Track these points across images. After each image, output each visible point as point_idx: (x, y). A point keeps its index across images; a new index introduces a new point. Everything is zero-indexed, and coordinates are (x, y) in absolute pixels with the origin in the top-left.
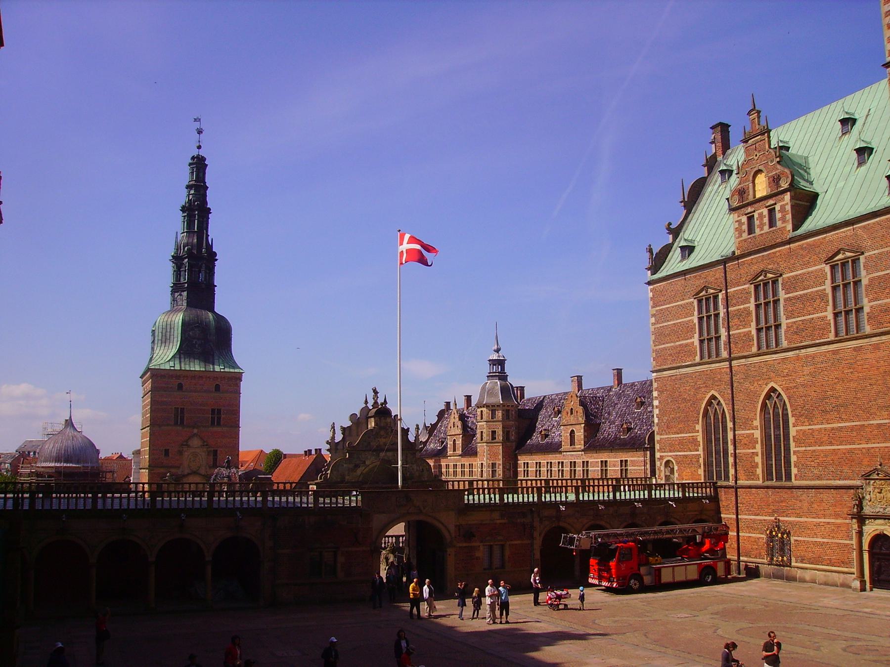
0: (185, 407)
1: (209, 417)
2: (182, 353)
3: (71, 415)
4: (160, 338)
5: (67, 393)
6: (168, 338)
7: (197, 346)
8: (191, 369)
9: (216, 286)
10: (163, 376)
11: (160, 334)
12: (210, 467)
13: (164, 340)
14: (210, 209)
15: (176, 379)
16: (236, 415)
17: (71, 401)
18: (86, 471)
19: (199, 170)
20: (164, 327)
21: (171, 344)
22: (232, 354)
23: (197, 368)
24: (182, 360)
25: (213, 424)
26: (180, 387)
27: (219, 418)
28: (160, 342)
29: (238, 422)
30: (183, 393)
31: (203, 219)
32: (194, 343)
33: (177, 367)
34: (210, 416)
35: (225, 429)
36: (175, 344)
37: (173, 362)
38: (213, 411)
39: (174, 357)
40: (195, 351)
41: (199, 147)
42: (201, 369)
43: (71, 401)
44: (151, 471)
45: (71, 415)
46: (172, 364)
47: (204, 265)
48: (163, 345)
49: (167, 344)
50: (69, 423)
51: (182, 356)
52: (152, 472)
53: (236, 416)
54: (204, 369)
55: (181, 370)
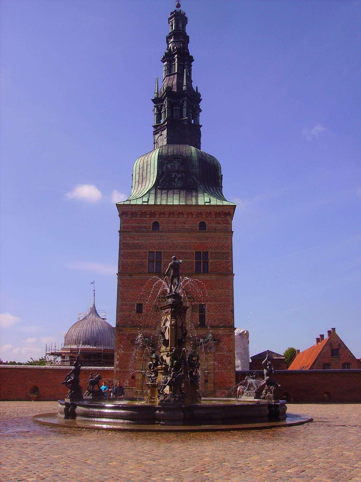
0: (163, 251)
2: (159, 189)
3: (94, 303)
4: (137, 180)
5: (92, 283)
6: (145, 177)
7: (176, 179)
8: (169, 204)
9: (201, 126)
10: (134, 214)
11: (137, 175)
12: (196, 327)
13: (141, 180)
14: (192, 57)
15: (150, 217)
17: (94, 291)
18: (100, 352)
20: (141, 166)
21: (148, 182)
22: (223, 196)
23: (176, 202)
24: (159, 195)
25: (198, 272)
26: (156, 225)
27: (206, 263)
28: (137, 184)
29: (230, 268)
30: (160, 234)
31: (184, 63)
32: (173, 176)
33: (152, 202)
34: (194, 260)
35: (214, 277)
36: (151, 180)
37: (147, 198)
39: (149, 192)
41: (178, 6)
42: (181, 204)
43: (94, 291)
44: (119, 331)
45: (94, 303)
46: (145, 199)
47: (185, 102)
48: (140, 185)
49: (144, 184)
50: (94, 311)
52: (120, 333)
54: (184, 204)
55: (155, 205)
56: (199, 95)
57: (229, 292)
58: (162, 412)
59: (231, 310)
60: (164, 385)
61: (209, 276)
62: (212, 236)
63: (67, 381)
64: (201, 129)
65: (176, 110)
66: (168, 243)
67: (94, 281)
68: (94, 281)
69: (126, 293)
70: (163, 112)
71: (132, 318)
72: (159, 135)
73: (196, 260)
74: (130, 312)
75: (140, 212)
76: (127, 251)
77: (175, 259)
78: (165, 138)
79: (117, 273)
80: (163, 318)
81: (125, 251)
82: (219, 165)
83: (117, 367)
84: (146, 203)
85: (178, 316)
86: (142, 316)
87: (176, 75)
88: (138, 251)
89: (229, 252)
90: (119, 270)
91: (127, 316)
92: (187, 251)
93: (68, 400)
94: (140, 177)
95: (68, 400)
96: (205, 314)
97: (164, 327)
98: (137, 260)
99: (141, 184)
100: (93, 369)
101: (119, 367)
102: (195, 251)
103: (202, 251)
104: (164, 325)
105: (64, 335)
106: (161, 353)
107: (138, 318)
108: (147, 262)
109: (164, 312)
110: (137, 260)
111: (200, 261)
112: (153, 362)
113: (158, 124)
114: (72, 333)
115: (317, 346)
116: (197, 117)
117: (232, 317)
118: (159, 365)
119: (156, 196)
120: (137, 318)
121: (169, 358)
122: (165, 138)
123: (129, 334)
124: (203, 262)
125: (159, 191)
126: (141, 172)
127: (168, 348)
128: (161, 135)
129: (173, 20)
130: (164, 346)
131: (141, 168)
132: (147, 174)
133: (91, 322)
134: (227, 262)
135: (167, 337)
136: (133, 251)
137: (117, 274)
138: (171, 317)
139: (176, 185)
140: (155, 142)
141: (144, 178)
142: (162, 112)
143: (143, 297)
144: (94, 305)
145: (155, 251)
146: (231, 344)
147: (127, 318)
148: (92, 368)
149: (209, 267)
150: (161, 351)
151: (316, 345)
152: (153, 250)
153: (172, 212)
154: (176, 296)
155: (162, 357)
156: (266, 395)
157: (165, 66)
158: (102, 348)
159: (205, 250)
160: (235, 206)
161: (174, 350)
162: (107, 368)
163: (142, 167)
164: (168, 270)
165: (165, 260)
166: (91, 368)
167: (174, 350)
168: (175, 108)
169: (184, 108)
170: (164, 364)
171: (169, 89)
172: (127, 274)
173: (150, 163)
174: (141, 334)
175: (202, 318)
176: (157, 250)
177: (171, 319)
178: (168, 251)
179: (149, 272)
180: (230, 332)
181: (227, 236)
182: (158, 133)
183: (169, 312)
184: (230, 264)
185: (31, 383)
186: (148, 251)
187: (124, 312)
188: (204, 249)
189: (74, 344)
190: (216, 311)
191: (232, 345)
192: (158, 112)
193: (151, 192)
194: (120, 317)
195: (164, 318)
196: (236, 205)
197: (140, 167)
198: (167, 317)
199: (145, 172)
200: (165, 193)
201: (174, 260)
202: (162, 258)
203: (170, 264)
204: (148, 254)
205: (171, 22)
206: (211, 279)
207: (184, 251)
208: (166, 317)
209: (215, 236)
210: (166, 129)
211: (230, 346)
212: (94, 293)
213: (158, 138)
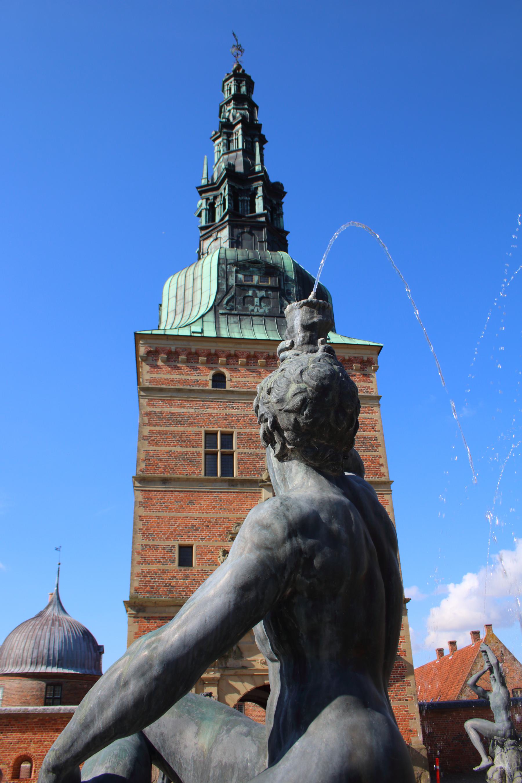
4: (172, 307)
14: (263, 136)
19: (239, 84)
31: (252, 139)
40: (253, 310)
43: (59, 564)
51: (223, 319)
53: (375, 454)
56: (281, 186)
64: (288, 237)
65: (243, 201)
67: (60, 547)
69: (155, 521)
70: (218, 206)
71: (170, 579)
72: (211, 239)
75: (186, 352)
78: (226, 241)
82: (327, 292)
84: (199, 335)
87: (240, 153)
88: (181, 429)
90: (139, 469)
91: (156, 574)
94: (178, 303)
98: (179, 449)
99: (179, 313)
100: (62, 712)
110: (179, 449)
113: (208, 223)
116: (279, 220)
119: (217, 326)
120: (180, 579)
122: (226, 241)
125: (223, 319)
126: (181, 292)
128: (216, 239)
129: (231, 82)
131: (181, 286)
132: (195, 294)
133: (50, 622)
134: (374, 457)
136: (171, 429)
139: (256, 310)
140: (204, 252)
141: (188, 302)
142: (216, 206)
145: (219, 430)
147: (156, 580)
148: (60, 709)
152: (215, 429)
153: (252, 353)
157: (218, 145)
160: (380, 348)
163: (183, 283)
166: (57, 709)
168: (242, 198)
169: (258, 198)
171: (230, 169)
173: (200, 274)
182: (211, 236)
186: (203, 430)
187: (149, 564)
191: (404, 639)
192: (208, 207)
193: (205, 318)
194: (140, 576)
196: (382, 347)
197: (179, 285)
199: (189, 293)
200: (235, 322)
205: (228, 85)
210: (228, 227)
212: (59, 568)
213: (210, 244)
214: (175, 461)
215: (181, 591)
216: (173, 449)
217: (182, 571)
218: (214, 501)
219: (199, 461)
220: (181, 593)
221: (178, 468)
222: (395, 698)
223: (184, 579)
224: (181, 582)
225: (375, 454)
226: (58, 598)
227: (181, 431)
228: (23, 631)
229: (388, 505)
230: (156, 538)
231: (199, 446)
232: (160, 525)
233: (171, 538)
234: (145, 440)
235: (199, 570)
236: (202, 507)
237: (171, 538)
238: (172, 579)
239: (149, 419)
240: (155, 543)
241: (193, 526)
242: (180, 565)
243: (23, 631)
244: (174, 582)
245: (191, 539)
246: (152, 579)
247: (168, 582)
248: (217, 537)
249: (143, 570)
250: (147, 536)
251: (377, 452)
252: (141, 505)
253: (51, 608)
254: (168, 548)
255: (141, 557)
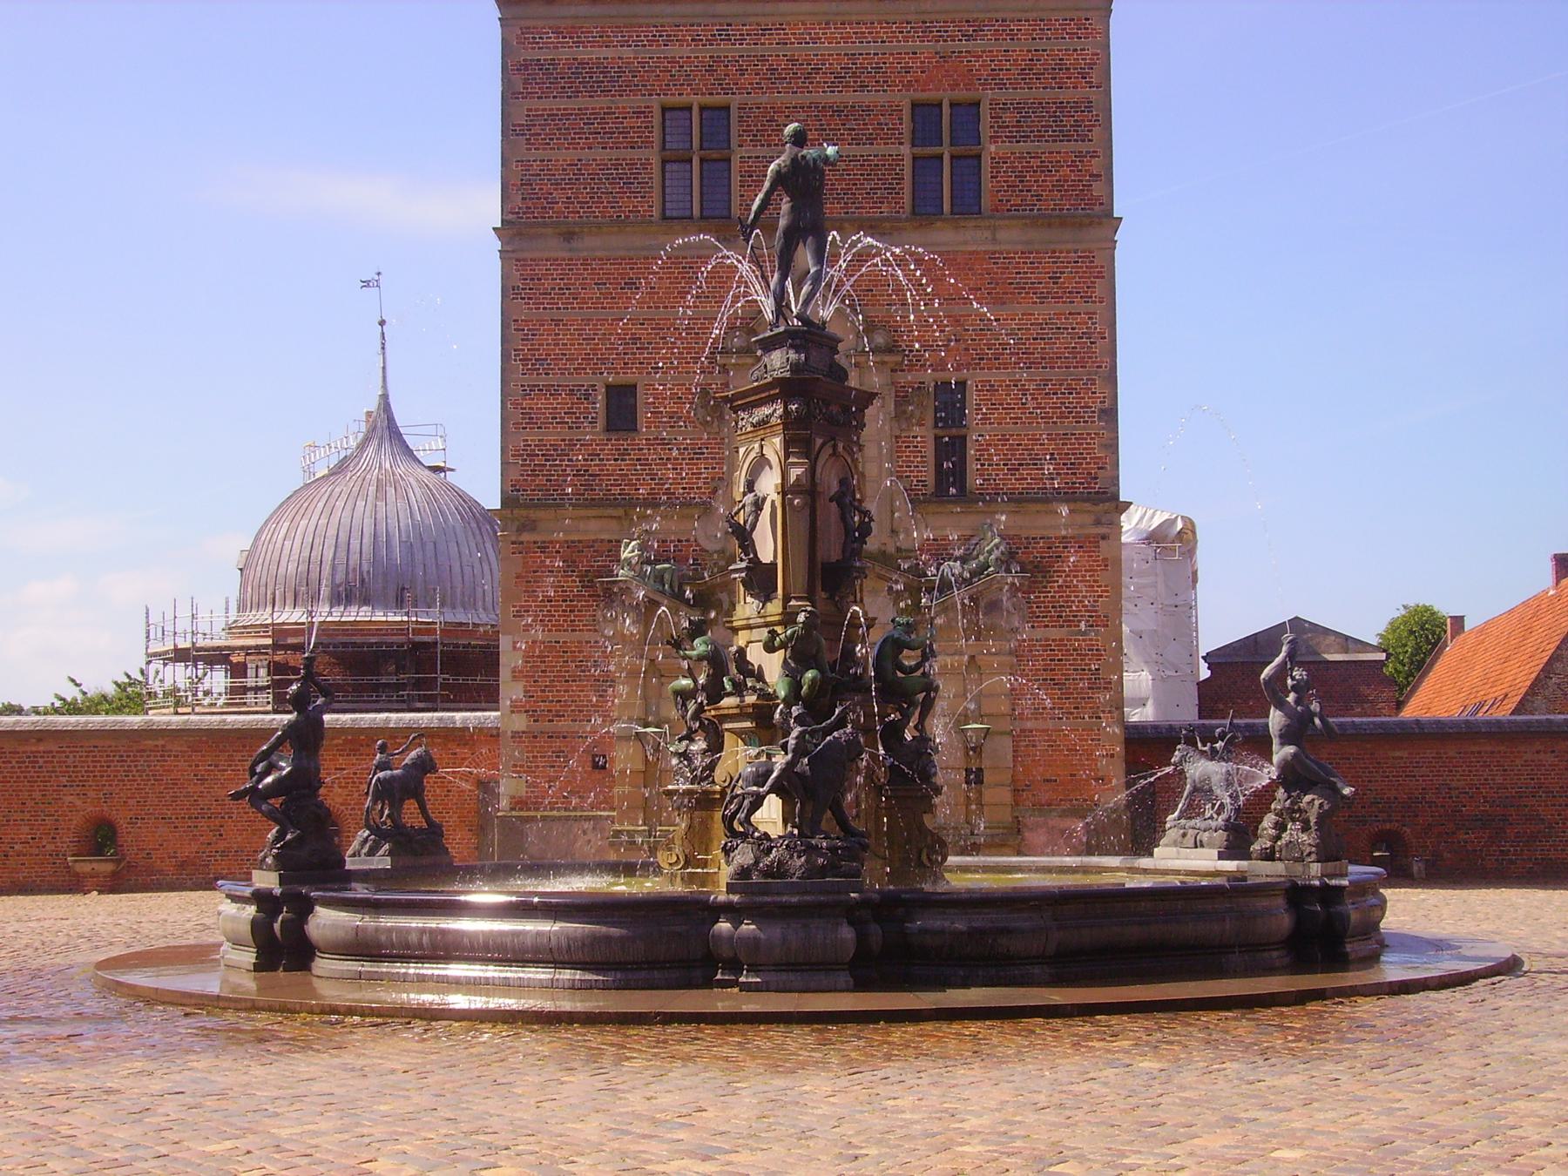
0: (735, 101)
1: (899, 158)
3: (385, 386)
5: (366, 284)
16: (1083, 139)
17: (382, 323)
25: (925, 210)
27: (968, 162)
29: (1097, 189)
34: (906, 150)
35: (1011, 237)
38: (925, 113)
43: (382, 323)
45: (385, 386)
52: (526, 537)
53: (1083, 147)
57: (1091, 315)
58: (748, 928)
59: (1102, 411)
60: (752, 794)
61: (987, 234)
62: (999, 16)
63: (260, 780)
66: (763, 59)
67: (379, 274)
68: (379, 274)
69: (549, 330)
73: (913, 145)
74: (569, 428)
76: (546, 104)
77: (799, 139)
79: (499, 226)
80: (742, 450)
81: (535, 103)
83: (513, 712)
85: (819, 441)
86: (635, 449)
88: (601, 102)
89: (1093, 98)
92: (866, 98)
93: (267, 880)
95: (267, 880)
96: (964, 431)
97: (749, 498)
101: (526, 712)
102: (908, 100)
103: (946, 97)
104: (750, 487)
105: (234, 559)
106: (735, 630)
107: (616, 460)
108: (655, 161)
109: (747, 420)
110: (600, 154)
111: (936, 150)
112: (695, 681)
114: (279, 545)
115: (1558, 597)
117: (1105, 446)
118: (729, 695)
120: (608, 460)
121: (779, 656)
123: (573, 542)
124: (952, 157)
127: (774, 608)
130: (749, 599)
133: (372, 489)
134: (1080, 155)
135: (767, 547)
136: (582, 102)
137: (494, 229)
138: (787, 444)
143: (637, 349)
144: (385, 397)
145: (696, 100)
146: (1100, 586)
147: (557, 462)
148: (387, 720)
149: (987, 184)
150: (735, 624)
151: (1551, 592)
154: (810, 336)
155: (742, 652)
156: (1278, 837)
158: (432, 616)
159: (962, 94)
161: (801, 618)
162: (465, 720)
164: (763, 201)
165: (743, 151)
166: (380, 719)
167: (801, 618)
170: (754, 689)
172: (550, 231)
174: (633, 543)
175: (951, 450)
176: (708, 100)
177: (787, 456)
178: (764, 99)
179: (668, 213)
180: (1098, 523)
181: (1082, 15)
183: (773, 421)
184: (1096, 165)
185: (78, 803)
186: (655, 103)
188: (954, 86)
189: (288, 602)
190: (1021, 418)
191: (1107, 591)
194: (523, 455)
195: (746, 454)
198: (762, 447)
201: (794, 144)
202: (734, 142)
203: (772, 166)
204: (656, 121)
206: (997, 248)
207: (850, 97)
208: (757, 446)
209: (1019, 15)
211: (1099, 596)
212: (383, 334)
214: (590, 184)
215: (611, 485)
216: (586, 154)
217: (613, 442)
218: (682, 278)
219: (647, 183)
220: (610, 490)
221: (597, 202)
222: (1072, 713)
223: (616, 460)
224: (610, 465)
225: (1083, 147)
226: (391, 420)
227: (602, 108)
228: (302, 511)
229: (1103, 277)
230: (552, 369)
231: (647, 144)
232: (561, 339)
233: (585, 369)
234: (517, 135)
235: (650, 439)
236: (655, 293)
237: (585, 369)
238: (592, 460)
239: (526, 82)
240: (553, 380)
241: (635, 339)
242: (610, 427)
243: (302, 511)
244: (595, 465)
245: (632, 368)
246: (549, 460)
247: (582, 465)
248: (689, 363)
249: (527, 440)
250: (532, 365)
251: (1089, 140)
252: (517, 294)
253: (371, 450)
254: (580, 390)
255: (522, 413)
